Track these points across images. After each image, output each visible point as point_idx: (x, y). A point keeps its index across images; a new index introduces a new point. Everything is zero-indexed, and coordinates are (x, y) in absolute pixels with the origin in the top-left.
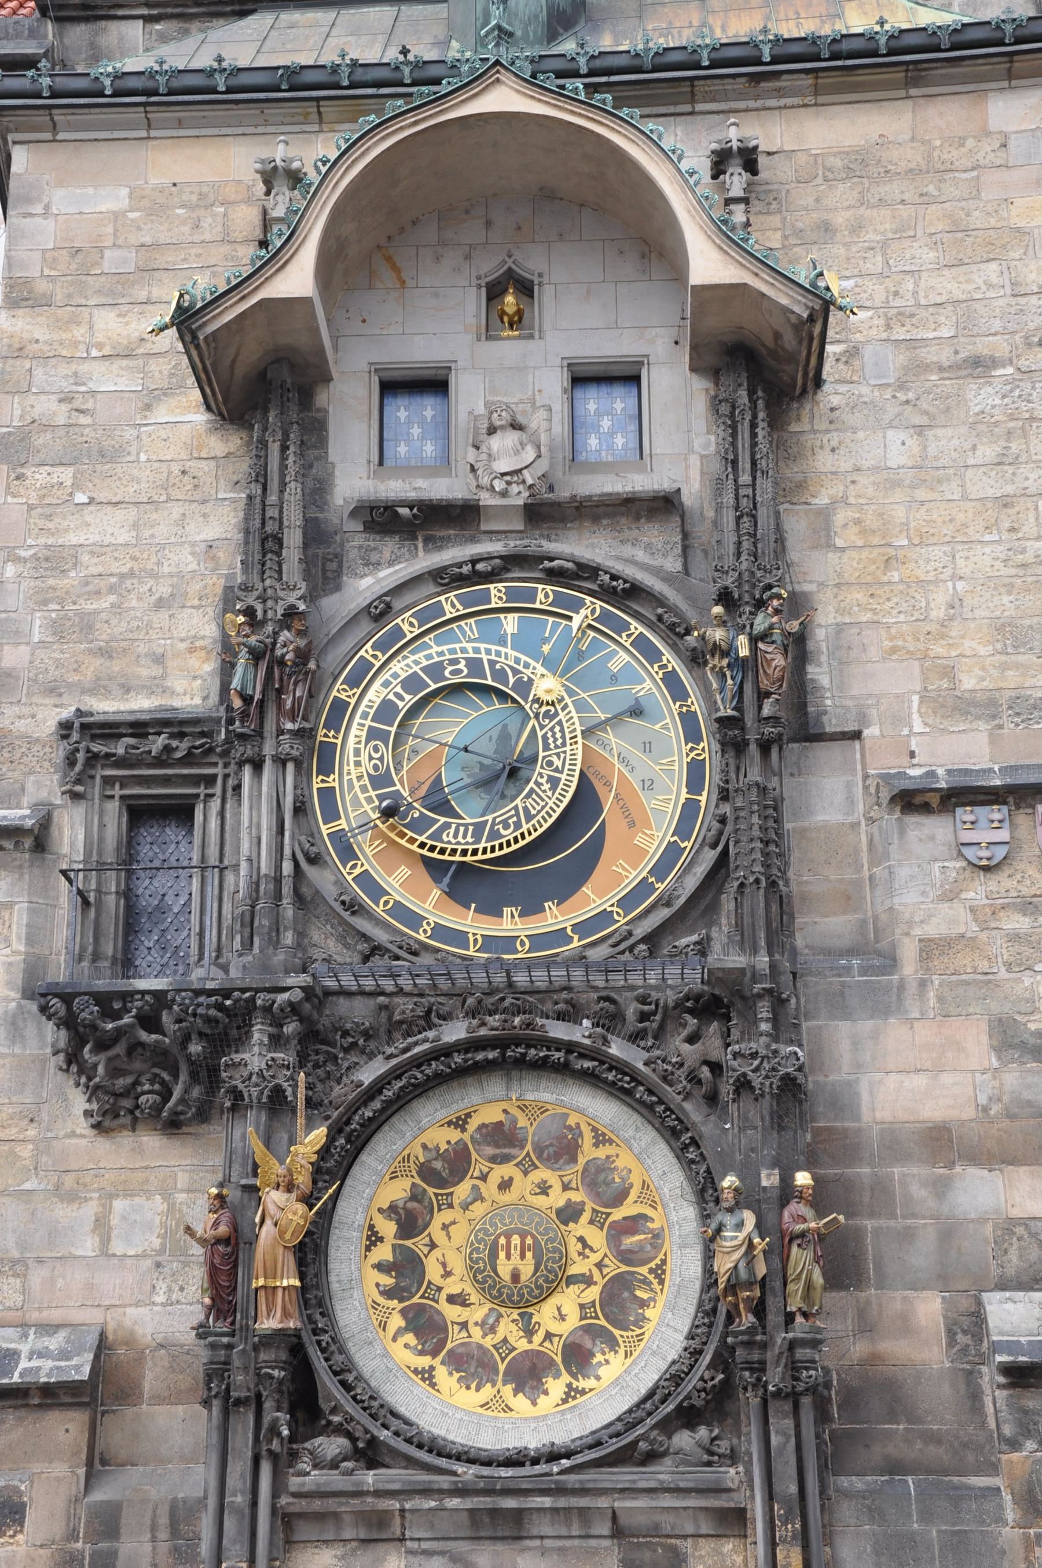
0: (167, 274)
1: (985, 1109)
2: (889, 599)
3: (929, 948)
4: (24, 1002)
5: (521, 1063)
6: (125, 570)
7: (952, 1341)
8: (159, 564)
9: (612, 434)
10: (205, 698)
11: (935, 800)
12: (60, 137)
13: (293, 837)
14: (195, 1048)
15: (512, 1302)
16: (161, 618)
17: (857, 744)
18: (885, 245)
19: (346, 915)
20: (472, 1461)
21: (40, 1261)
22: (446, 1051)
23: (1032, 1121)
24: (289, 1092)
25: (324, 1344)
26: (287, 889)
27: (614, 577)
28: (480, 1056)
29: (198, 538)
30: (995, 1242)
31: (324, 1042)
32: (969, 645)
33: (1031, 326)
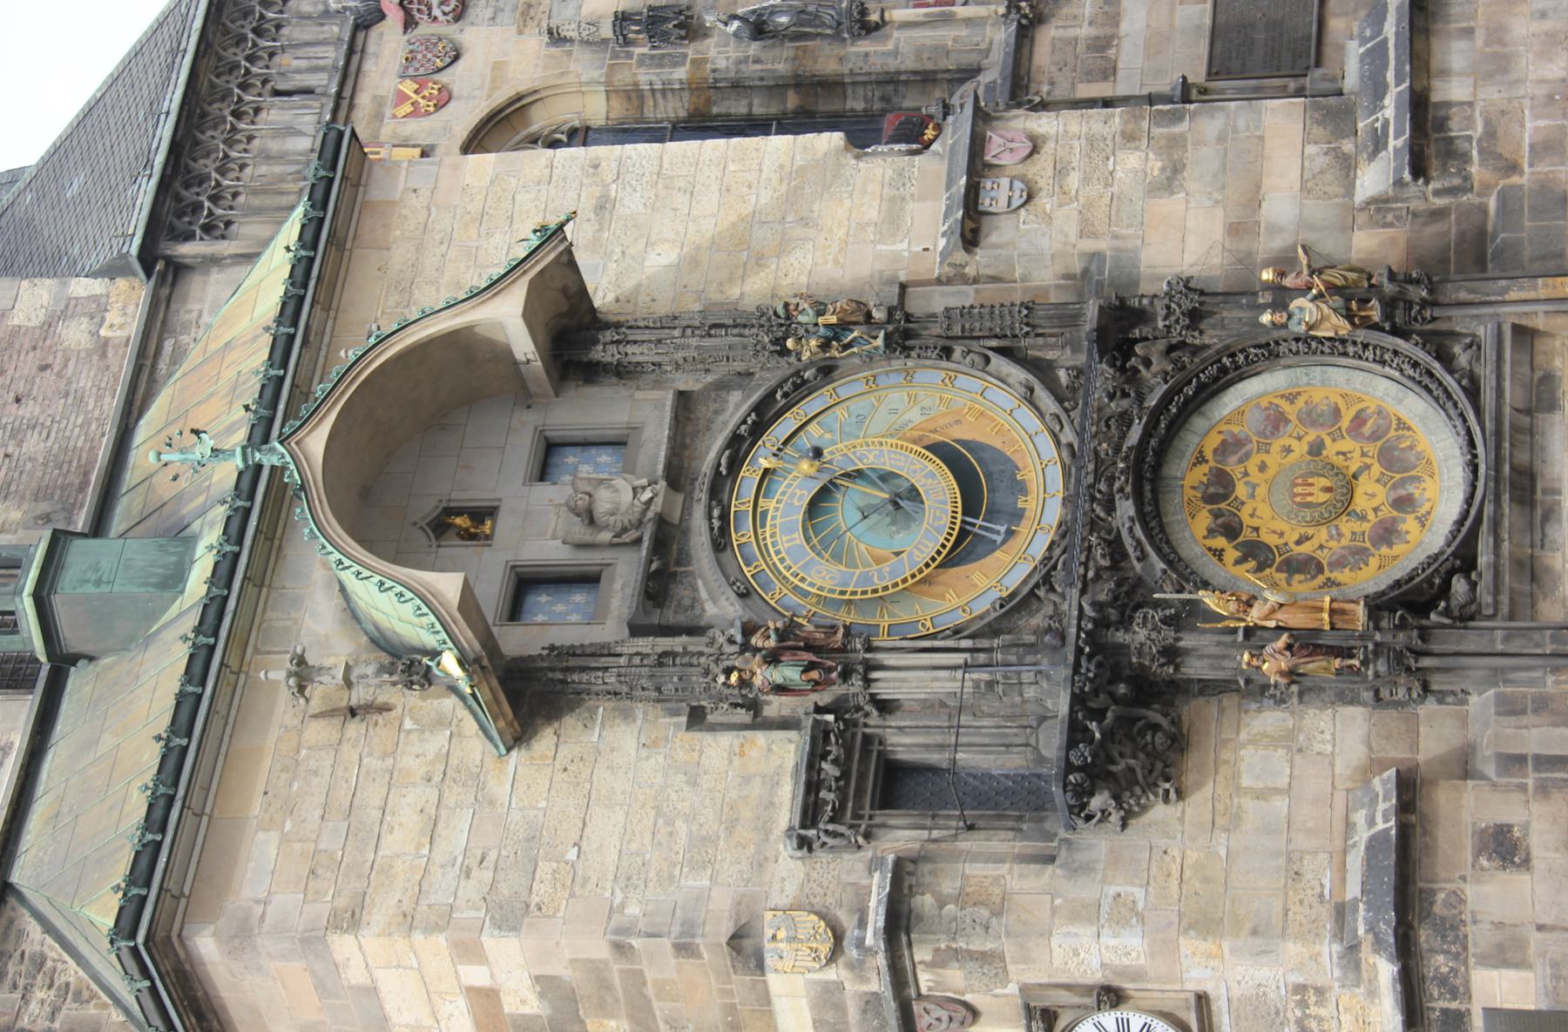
0: (358, 794)
1: (1217, 202)
4: (1057, 863)
5: (1157, 467)
7: (1391, 225)
8: (652, 786)
9: (597, 465)
10: (790, 741)
11: (970, 224)
16: (706, 782)
17: (910, 290)
21: (1289, 841)
22: (1142, 516)
24: (1167, 612)
26: (985, 643)
27: (744, 422)
28: (1148, 495)
29: (633, 754)
33: (579, 173)
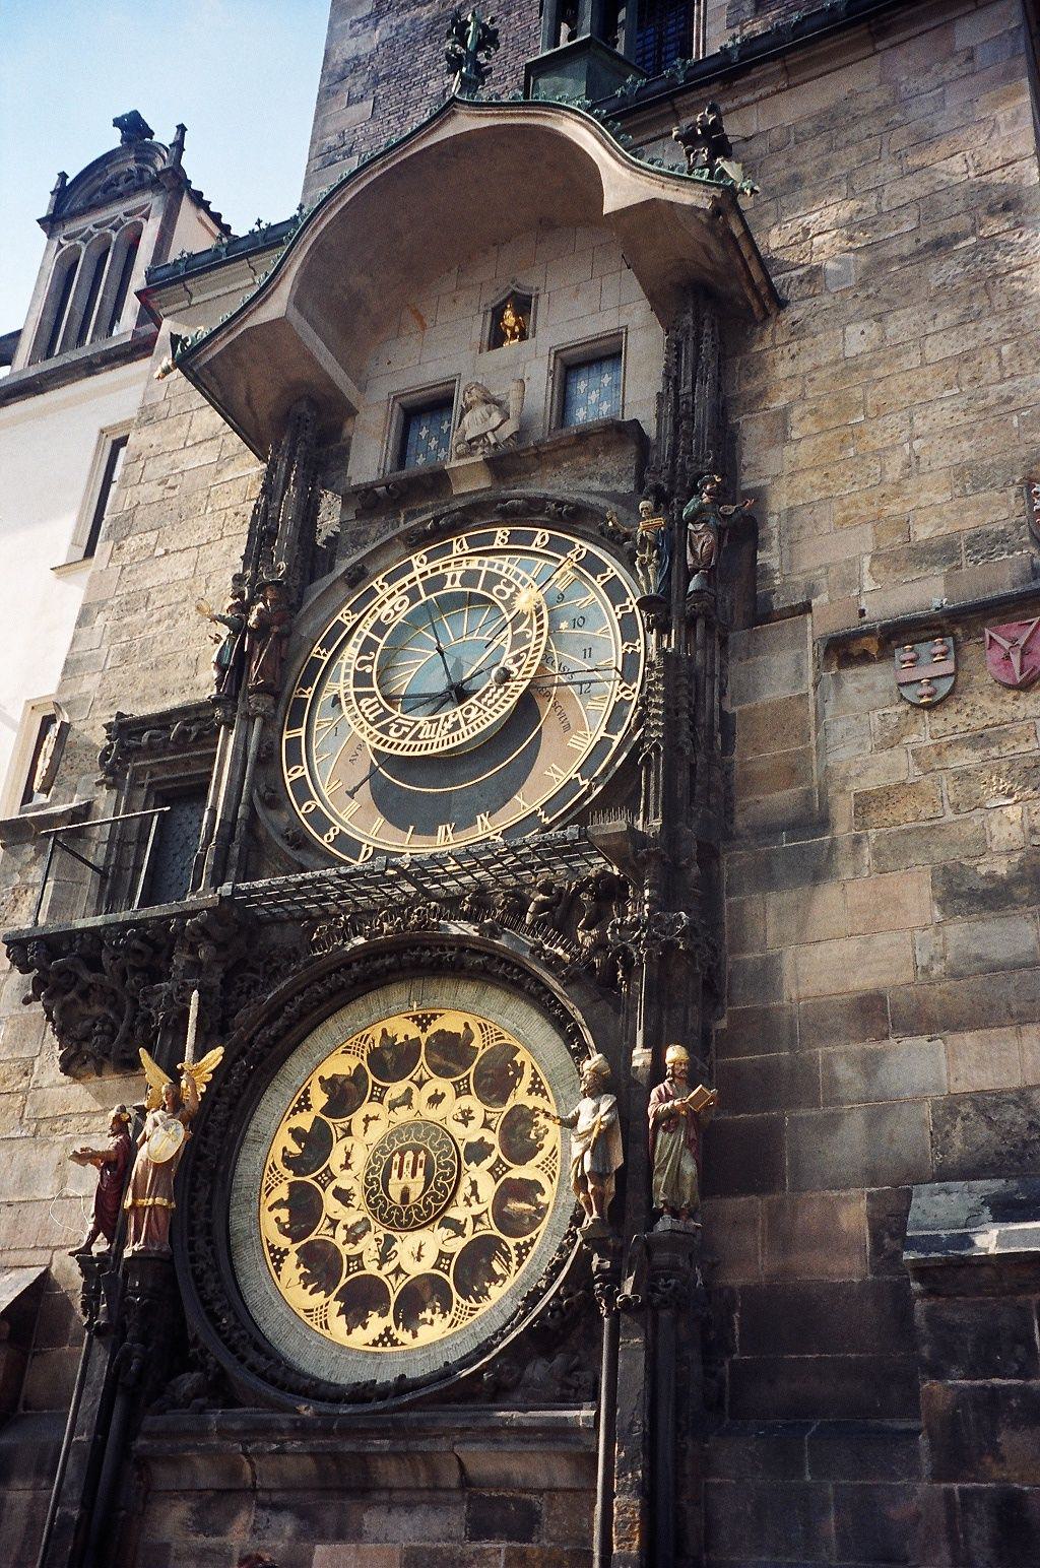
2: (843, 475)
3: (865, 803)
6: (180, 599)
9: (599, 403)
12: (193, 302)
13: (253, 784)
14: (130, 982)
15: (401, 1225)
18: (849, 176)
19: (288, 850)
20: (322, 1398)
23: (981, 978)
25: (198, 1272)
26: (240, 829)
27: (560, 504)
30: (935, 1125)
31: (256, 971)
32: (924, 498)
33: (995, 195)
